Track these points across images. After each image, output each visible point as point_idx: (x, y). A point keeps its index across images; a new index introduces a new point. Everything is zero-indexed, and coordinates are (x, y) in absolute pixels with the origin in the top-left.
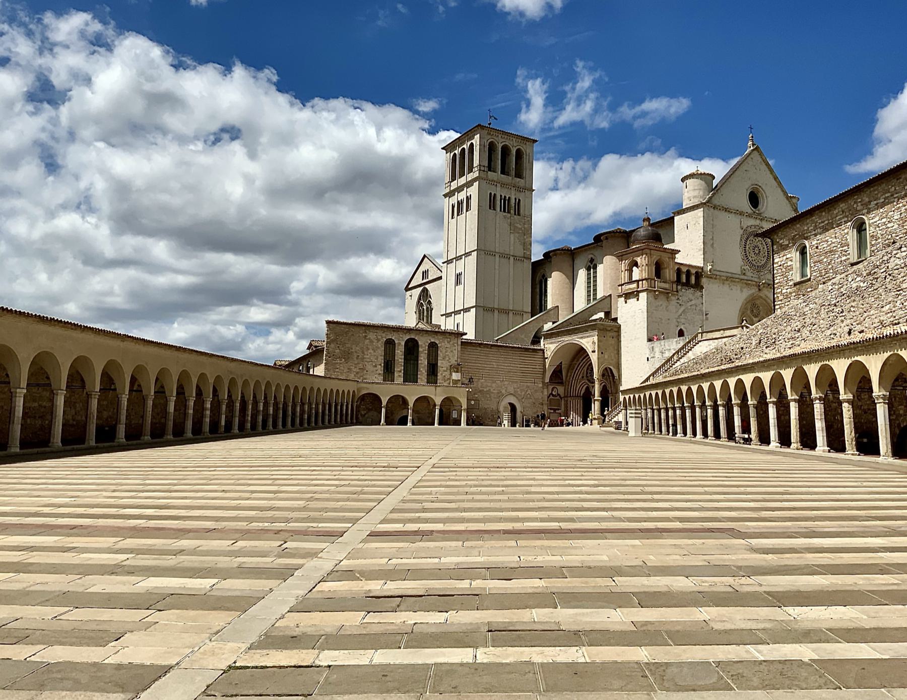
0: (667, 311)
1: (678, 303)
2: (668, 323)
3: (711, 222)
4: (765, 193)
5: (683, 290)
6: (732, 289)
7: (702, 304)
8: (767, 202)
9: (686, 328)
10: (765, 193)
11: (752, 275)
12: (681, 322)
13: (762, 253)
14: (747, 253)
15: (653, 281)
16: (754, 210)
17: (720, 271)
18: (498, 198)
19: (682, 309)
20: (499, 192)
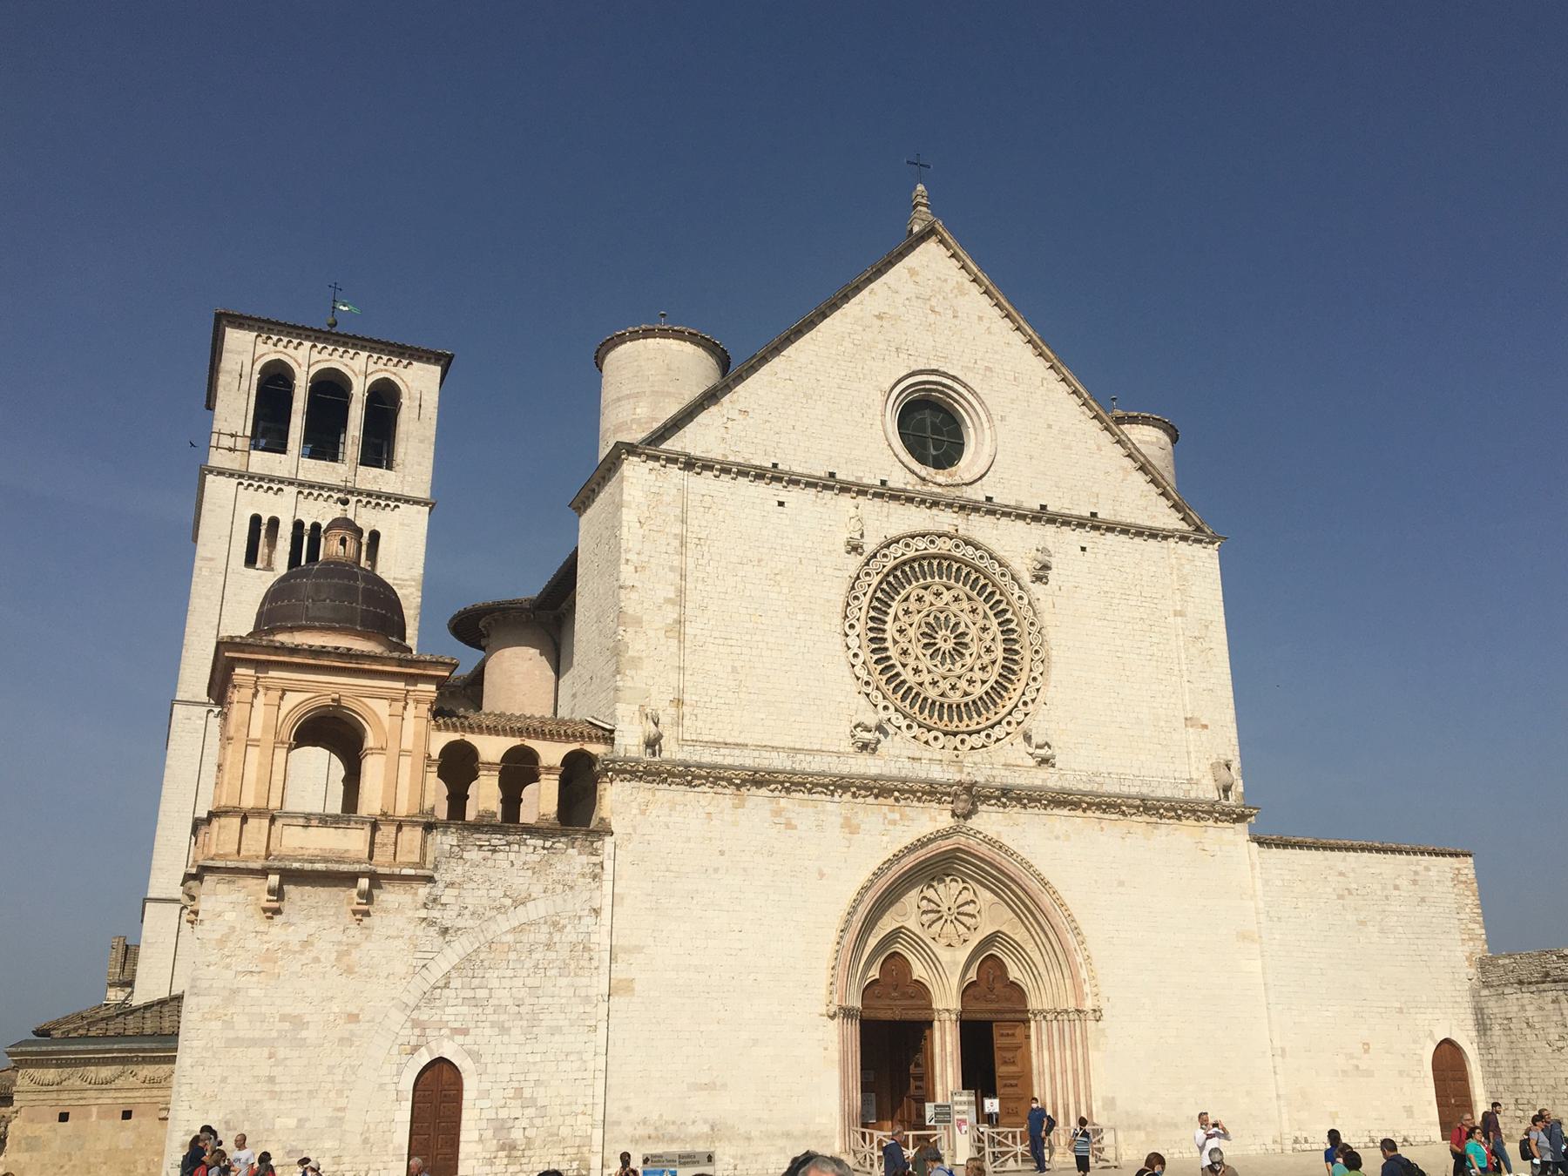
0: (349, 970)
1: (432, 923)
2: (345, 1041)
3: (677, 529)
4: (982, 403)
5: (473, 855)
6: (789, 826)
7: (596, 912)
8: (994, 440)
9: (475, 1056)
10: (982, 403)
11: (916, 749)
12: (441, 1025)
13: (974, 648)
14: (893, 652)
15: (266, 822)
16: (924, 471)
17: (717, 745)
18: (285, 531)
19: (460, 947)
20: (284, 508)
